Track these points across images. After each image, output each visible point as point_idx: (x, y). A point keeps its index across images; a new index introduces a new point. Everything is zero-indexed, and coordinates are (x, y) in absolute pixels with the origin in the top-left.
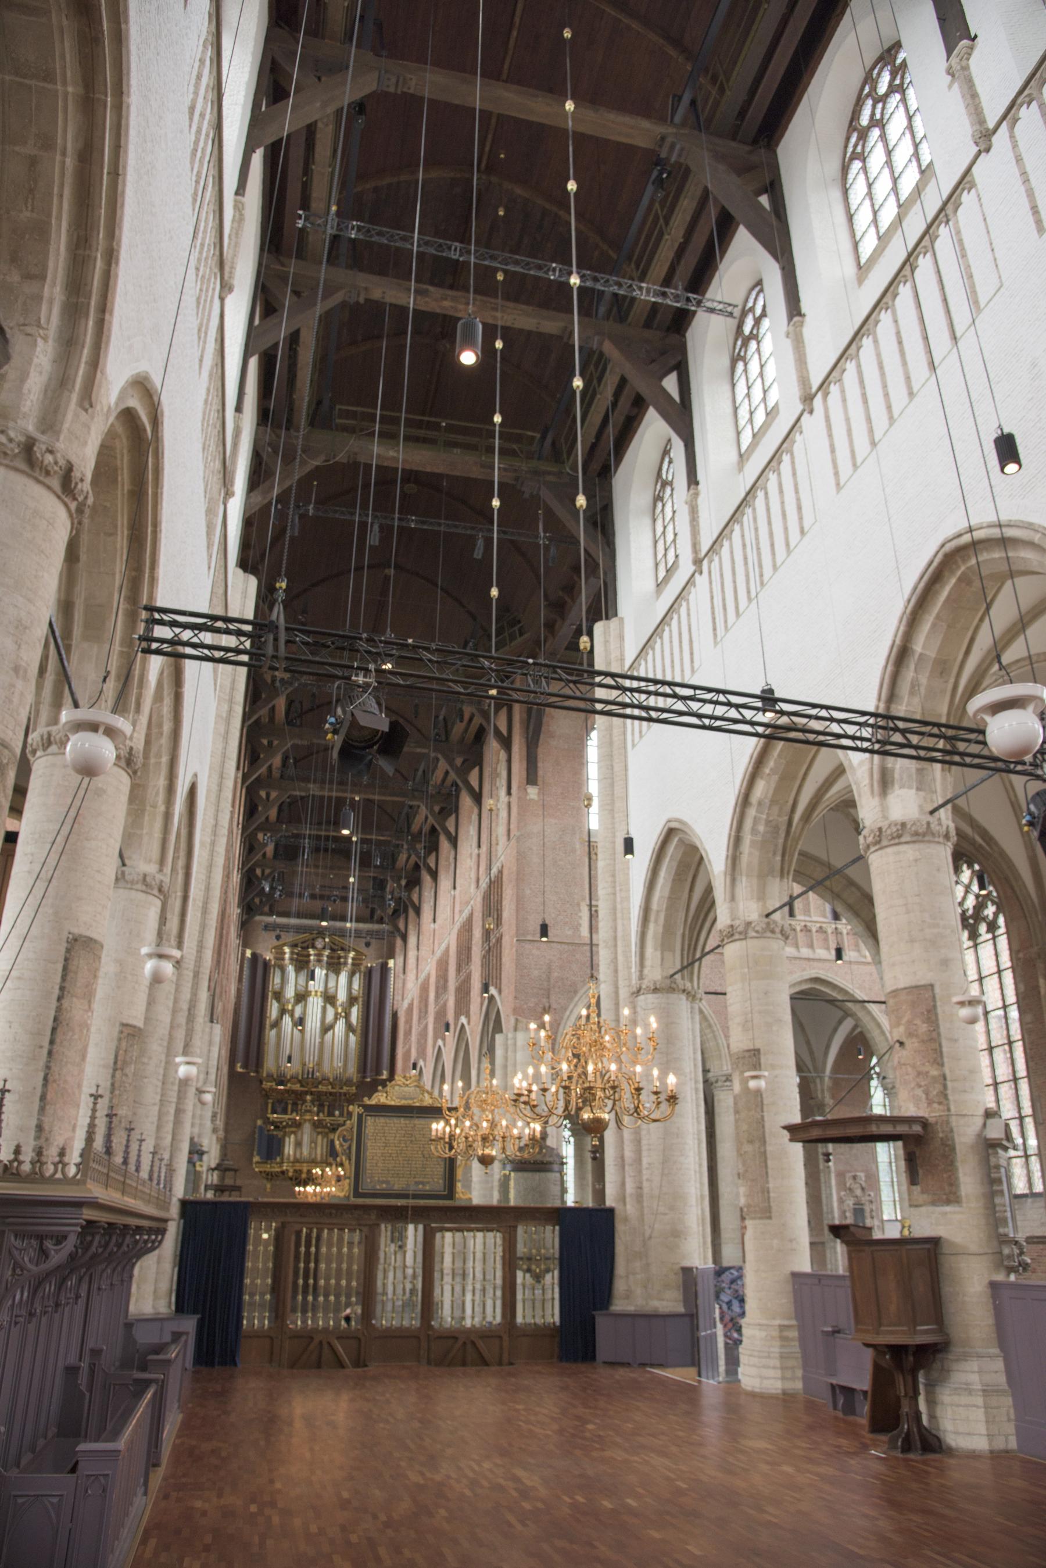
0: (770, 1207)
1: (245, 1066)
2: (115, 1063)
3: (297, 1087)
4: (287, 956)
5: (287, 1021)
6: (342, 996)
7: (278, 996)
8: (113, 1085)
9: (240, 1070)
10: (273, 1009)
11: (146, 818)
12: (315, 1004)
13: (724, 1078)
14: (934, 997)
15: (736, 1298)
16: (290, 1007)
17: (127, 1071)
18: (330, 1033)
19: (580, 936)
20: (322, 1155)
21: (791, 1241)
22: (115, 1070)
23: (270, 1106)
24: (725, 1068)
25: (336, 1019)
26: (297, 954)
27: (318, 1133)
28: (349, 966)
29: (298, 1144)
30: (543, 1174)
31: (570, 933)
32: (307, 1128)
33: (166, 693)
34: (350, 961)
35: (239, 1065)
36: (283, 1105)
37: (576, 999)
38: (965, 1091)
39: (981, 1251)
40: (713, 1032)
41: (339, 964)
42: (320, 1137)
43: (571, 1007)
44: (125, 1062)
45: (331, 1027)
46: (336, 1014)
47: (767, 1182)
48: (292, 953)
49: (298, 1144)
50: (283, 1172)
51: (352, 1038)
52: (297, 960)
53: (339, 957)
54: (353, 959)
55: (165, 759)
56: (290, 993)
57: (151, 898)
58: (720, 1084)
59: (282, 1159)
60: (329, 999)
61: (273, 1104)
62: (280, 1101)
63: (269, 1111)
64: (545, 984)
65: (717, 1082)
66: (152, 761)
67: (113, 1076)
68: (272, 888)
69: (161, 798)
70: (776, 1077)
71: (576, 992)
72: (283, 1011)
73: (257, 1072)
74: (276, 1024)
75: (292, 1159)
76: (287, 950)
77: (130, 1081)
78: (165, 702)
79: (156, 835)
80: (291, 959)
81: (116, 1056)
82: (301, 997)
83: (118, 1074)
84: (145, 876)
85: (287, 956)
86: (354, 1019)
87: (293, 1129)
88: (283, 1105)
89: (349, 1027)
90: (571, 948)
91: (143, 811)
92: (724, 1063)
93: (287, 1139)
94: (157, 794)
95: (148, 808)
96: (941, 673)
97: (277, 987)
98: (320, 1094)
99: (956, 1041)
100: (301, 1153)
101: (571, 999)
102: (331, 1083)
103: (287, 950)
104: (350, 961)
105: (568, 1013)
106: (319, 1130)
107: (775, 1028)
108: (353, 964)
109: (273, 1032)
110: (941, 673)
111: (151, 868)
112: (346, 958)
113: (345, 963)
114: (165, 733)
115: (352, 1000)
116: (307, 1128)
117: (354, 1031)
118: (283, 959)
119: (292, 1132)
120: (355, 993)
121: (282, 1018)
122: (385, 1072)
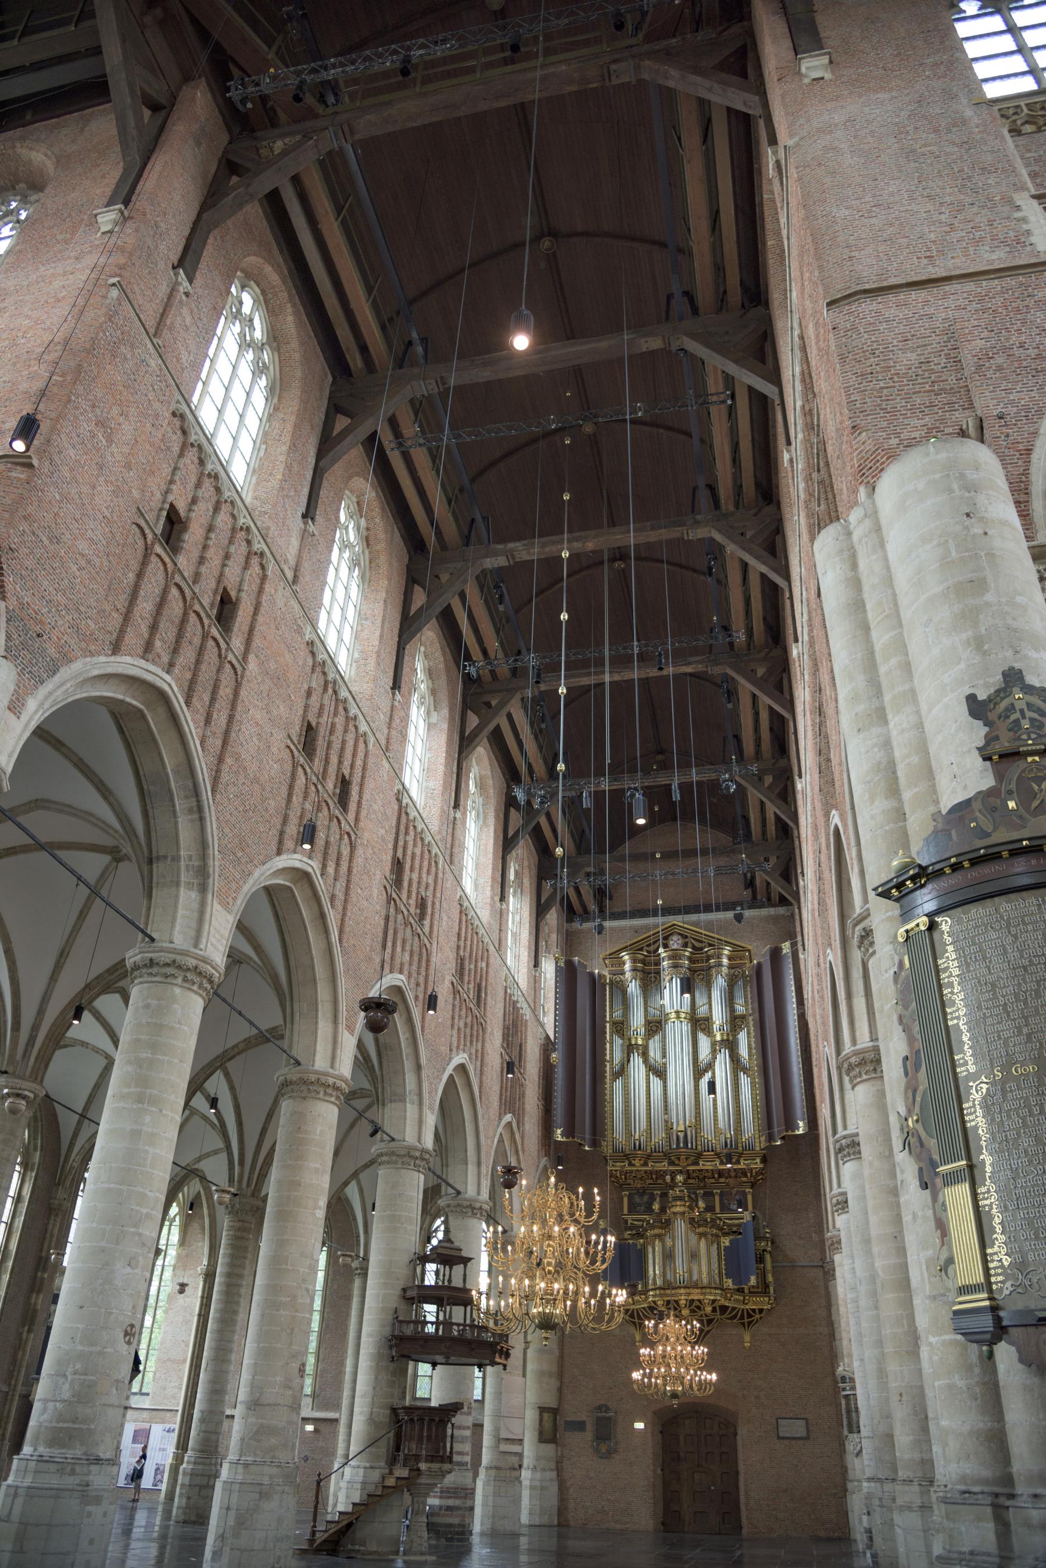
1: (569, 1132)
3: (664, 1166)
4: (627, 966)
5: (637, 1068)
6: (718, 1016)
7: (621, 1027)
9: (560, 1138)
10: (614, 1049)
12: (678, 1032)
16: (640, 1042)
18: (708, 1076)
20: (709, 1273)
23: (626, 1200)
25: (714, 1052)
26: (643, 962)
27: (701, 1235)
28: (725, 970)
29: (668, 1256)
32: (680, 1226)
34: (725, 961)
35: (559, 1131)
36: (646, 1198)
41: (710, 968)
42: (703, 1243)
45: (710, 1066)
46: (714, 1044)
48: (634, 961)
49: (668, 1256)
50: (651, 1309)
51: (745, 1081)
52: (643, 971)
53: (708, 958)
54: (730, 958)
56: (637, 1020)
59: (646, 1284)
60: (699, 1024)
61: (630, 1197)
62: (642, 1192)
63: (626, 1211)
68: (529, 793)
72: (630, 1049)
73: (595, 1143)
74: (621, 1072)
75: (659, 1282)
76: (626, 957)
80: (634, 969)
82: (655, 1026)
85: (627, 966)
86: (743, 1051)
87: (657, 1231)
88: (646, 1198)
89: (736, 1063)
93: (650, 1249)
97: (618, 1015)
98: (702, 1176)
100: (675, 1273)
102: (718, 1156)
103: (626, 957)
104: (725, 961)
106: (701, 1230)
108: (730, 967)
109: (618, 1084)
112: (719, 956)
113: (720, 965)
115: (735, 1022)
116: (680, 1226)
117: (745, 1070)
118: (623, 973)
119: (659, 1236)
120: (740, 1009)
121: (629, 1061)
122: (801, 1124)
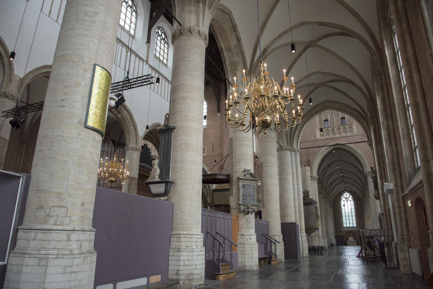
0: (264, 204)
2: (129, 184)
8: (128, 189)
11: (131, 136)
13: (368, 173)
14: (232, 141)
15: (377, 240)
17: (132, 186)
19: (316, 138)
21: (269, 213)
22: (129, 186)
24: (368, 170)
30: (308, 206)
31: (313, 138)
33: (123, 110)
37: (317, 156)
38: (237, 165)
39: (236, 208)
40: (363, 159)
43: (316, 159)
44: (131, 184)
47: (264, 198)
55: (131, 123)
57: (134, 151)
58: (367, 175)
64: (308, 153)
65: (367, 174)
66: (128, 124)
67: (128, 187)
69: (133, 131)
70: (266, 169)
71: (317, 154)
77: (133, 188)
78: (125, 112)
79: (134, 139)
81: (129, 183)
83: (130, 187)
84: (132, 147)
90: (314, 142)
91: (130, 134)
92: (368, 168)
94: (132, 130)
95: (131, 134)
96: (229, 51)
99: (236, 152)
101: (315, 156)
105: (315, 160)
107: (266, 156)
110: (229, 51)
111: (134, 146)
114: (129, 118)
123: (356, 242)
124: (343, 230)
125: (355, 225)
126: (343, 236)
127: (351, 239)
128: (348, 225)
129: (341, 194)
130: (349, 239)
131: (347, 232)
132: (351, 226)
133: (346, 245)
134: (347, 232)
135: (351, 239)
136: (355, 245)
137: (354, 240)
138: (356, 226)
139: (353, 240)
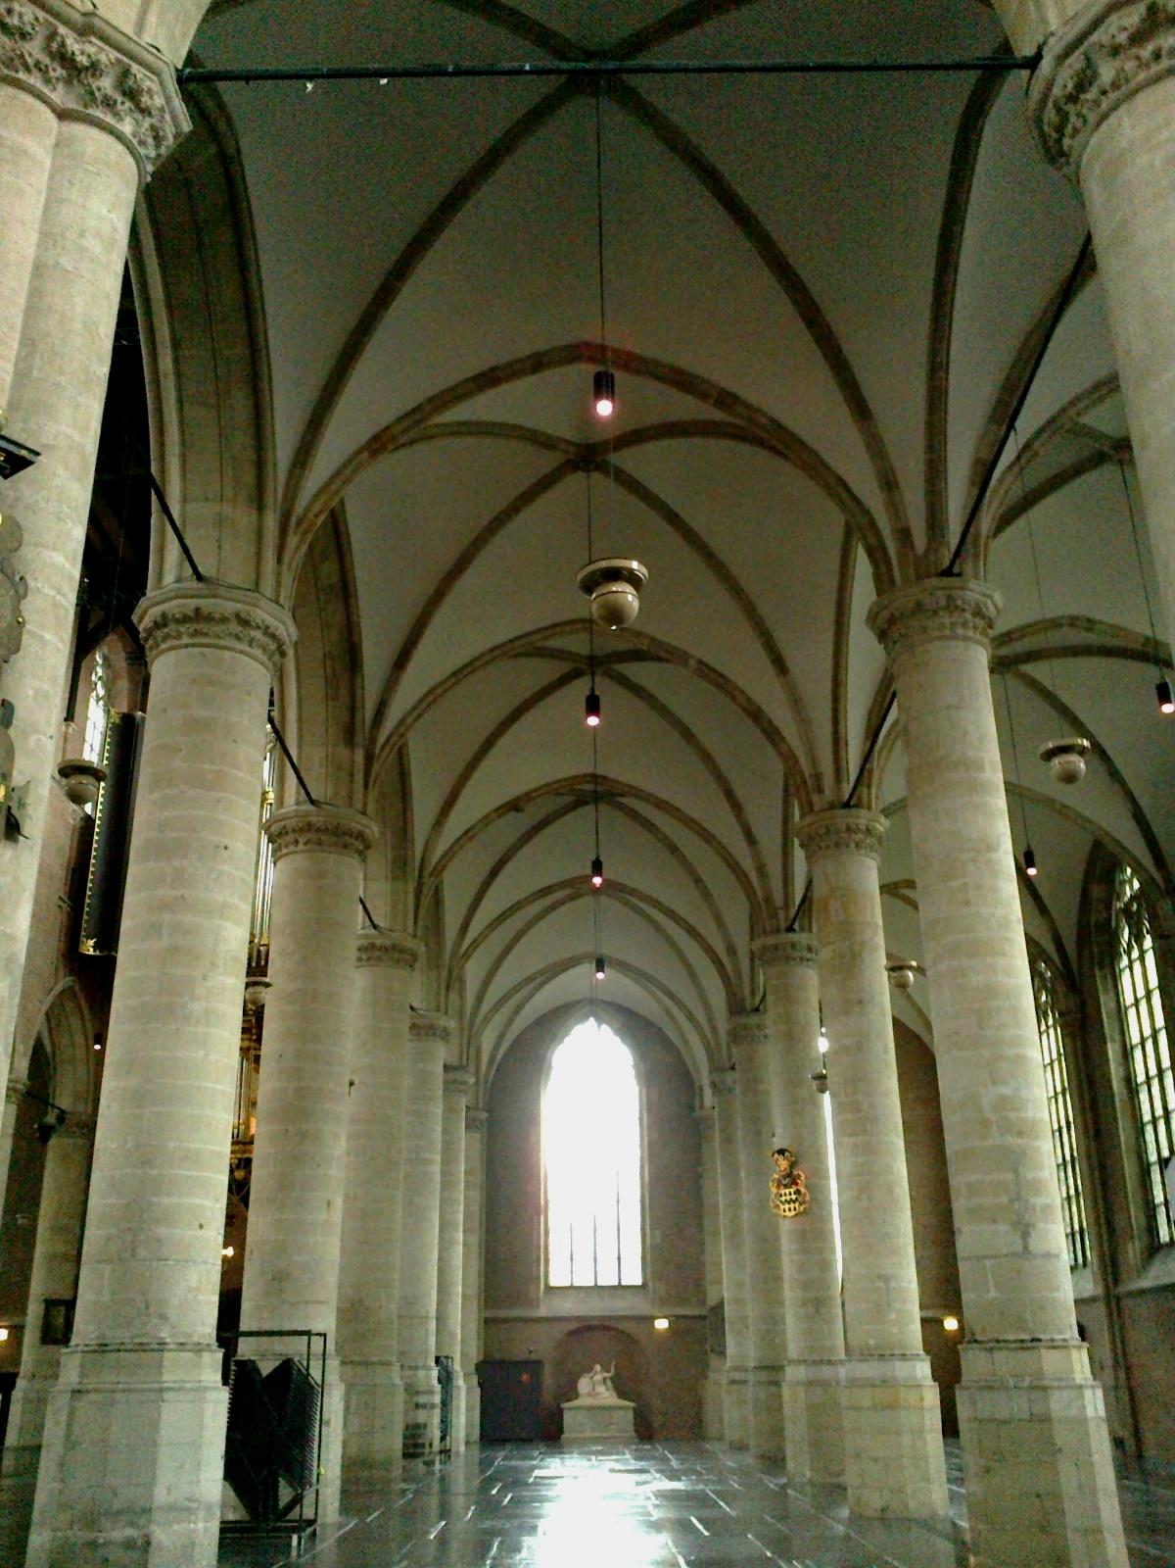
35: (91, 942)
123: (630, 1415)
124: (543, 1311)
125: (633, 1276)
126: (539, 1362)
127: (595, 1389)
128: (585, 1280)
129: (552, 1024)
130: (584, 1384)
131: (574, 1326)
132: (608, 1279)
133: (550, 1435)
134: (571, 1333)
135: (595, 1389)
136: (626, 1443)
137: (622, 1394)
138: (639, 1282)
139: (606, 1396)
